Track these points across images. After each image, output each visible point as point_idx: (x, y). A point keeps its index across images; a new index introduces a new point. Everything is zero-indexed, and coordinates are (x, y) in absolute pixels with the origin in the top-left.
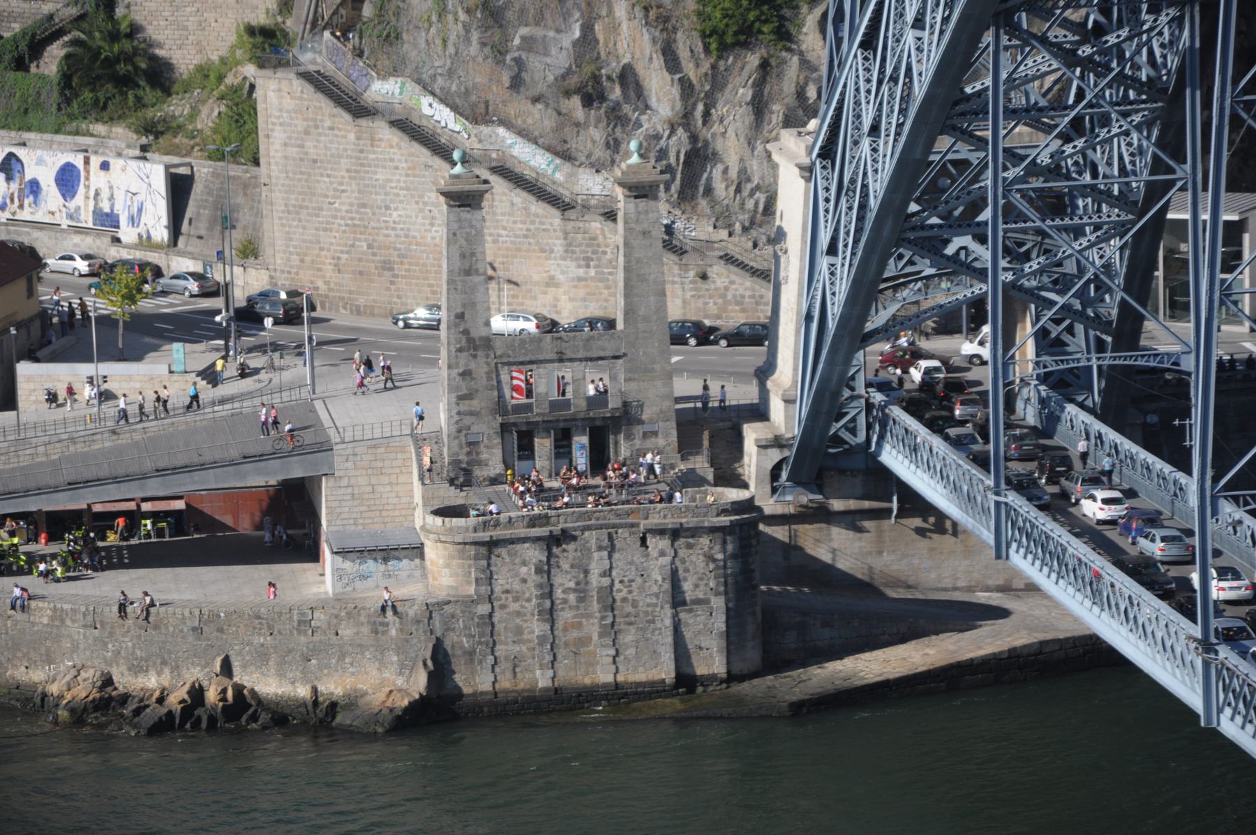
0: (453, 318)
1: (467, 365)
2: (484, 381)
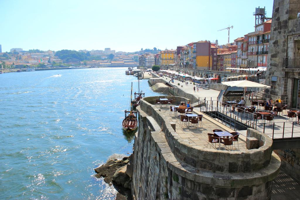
0: (274, 12)
1: (276, 38)
2: (282, 46)
